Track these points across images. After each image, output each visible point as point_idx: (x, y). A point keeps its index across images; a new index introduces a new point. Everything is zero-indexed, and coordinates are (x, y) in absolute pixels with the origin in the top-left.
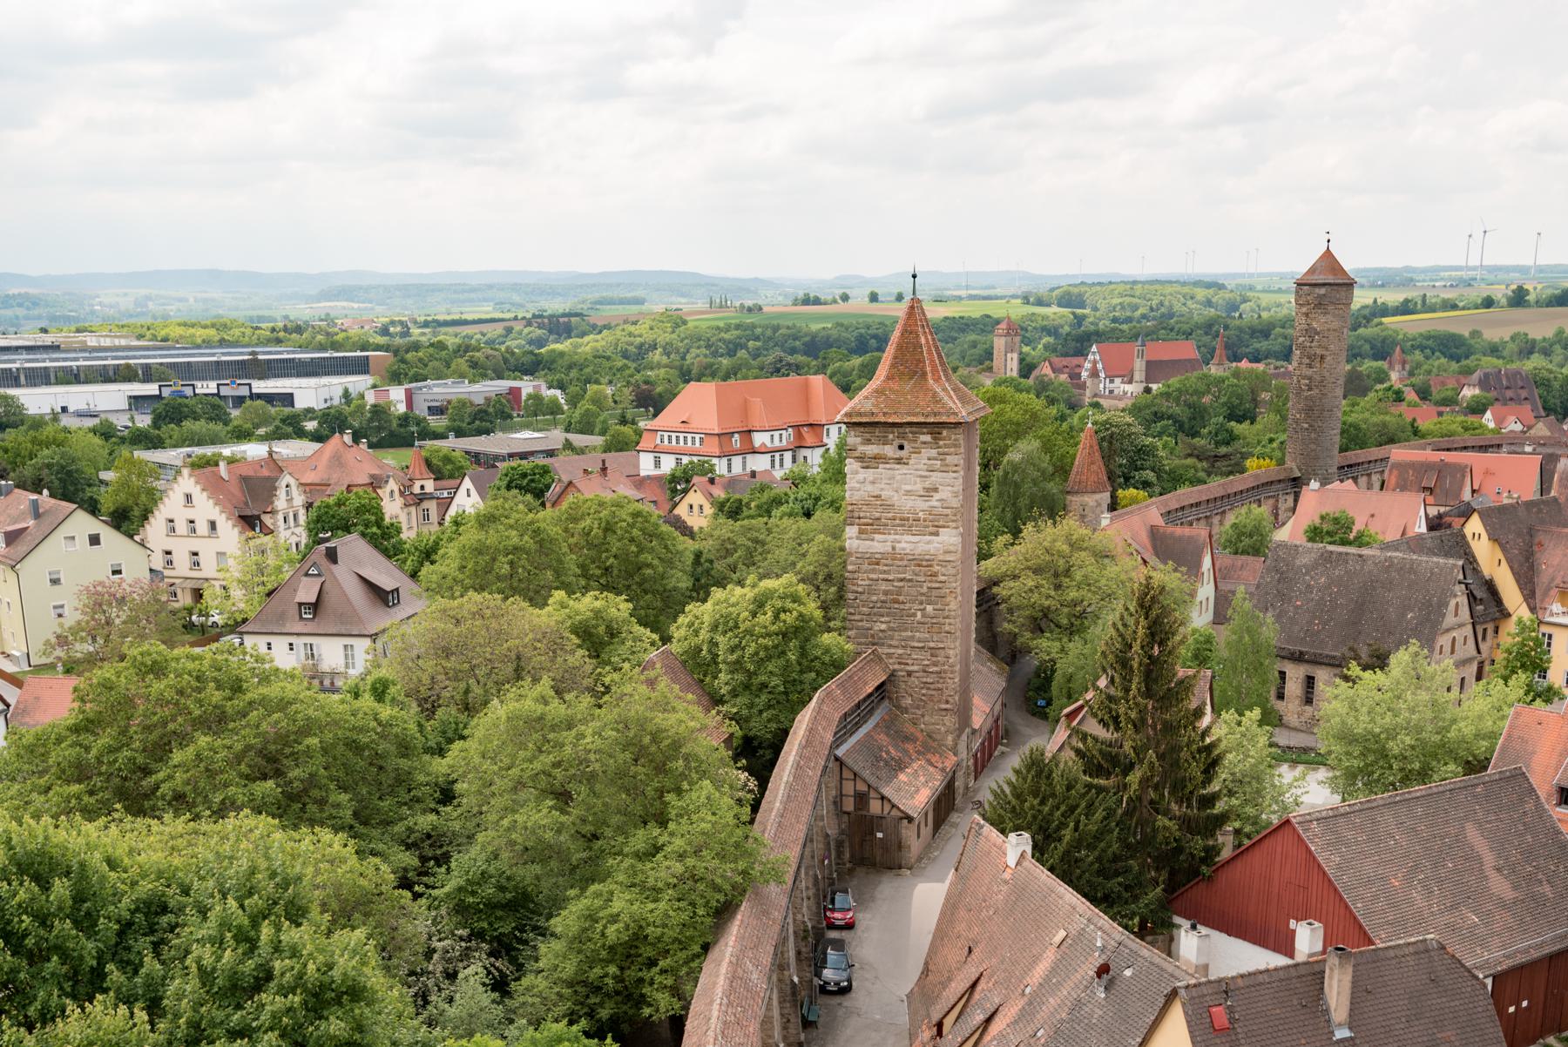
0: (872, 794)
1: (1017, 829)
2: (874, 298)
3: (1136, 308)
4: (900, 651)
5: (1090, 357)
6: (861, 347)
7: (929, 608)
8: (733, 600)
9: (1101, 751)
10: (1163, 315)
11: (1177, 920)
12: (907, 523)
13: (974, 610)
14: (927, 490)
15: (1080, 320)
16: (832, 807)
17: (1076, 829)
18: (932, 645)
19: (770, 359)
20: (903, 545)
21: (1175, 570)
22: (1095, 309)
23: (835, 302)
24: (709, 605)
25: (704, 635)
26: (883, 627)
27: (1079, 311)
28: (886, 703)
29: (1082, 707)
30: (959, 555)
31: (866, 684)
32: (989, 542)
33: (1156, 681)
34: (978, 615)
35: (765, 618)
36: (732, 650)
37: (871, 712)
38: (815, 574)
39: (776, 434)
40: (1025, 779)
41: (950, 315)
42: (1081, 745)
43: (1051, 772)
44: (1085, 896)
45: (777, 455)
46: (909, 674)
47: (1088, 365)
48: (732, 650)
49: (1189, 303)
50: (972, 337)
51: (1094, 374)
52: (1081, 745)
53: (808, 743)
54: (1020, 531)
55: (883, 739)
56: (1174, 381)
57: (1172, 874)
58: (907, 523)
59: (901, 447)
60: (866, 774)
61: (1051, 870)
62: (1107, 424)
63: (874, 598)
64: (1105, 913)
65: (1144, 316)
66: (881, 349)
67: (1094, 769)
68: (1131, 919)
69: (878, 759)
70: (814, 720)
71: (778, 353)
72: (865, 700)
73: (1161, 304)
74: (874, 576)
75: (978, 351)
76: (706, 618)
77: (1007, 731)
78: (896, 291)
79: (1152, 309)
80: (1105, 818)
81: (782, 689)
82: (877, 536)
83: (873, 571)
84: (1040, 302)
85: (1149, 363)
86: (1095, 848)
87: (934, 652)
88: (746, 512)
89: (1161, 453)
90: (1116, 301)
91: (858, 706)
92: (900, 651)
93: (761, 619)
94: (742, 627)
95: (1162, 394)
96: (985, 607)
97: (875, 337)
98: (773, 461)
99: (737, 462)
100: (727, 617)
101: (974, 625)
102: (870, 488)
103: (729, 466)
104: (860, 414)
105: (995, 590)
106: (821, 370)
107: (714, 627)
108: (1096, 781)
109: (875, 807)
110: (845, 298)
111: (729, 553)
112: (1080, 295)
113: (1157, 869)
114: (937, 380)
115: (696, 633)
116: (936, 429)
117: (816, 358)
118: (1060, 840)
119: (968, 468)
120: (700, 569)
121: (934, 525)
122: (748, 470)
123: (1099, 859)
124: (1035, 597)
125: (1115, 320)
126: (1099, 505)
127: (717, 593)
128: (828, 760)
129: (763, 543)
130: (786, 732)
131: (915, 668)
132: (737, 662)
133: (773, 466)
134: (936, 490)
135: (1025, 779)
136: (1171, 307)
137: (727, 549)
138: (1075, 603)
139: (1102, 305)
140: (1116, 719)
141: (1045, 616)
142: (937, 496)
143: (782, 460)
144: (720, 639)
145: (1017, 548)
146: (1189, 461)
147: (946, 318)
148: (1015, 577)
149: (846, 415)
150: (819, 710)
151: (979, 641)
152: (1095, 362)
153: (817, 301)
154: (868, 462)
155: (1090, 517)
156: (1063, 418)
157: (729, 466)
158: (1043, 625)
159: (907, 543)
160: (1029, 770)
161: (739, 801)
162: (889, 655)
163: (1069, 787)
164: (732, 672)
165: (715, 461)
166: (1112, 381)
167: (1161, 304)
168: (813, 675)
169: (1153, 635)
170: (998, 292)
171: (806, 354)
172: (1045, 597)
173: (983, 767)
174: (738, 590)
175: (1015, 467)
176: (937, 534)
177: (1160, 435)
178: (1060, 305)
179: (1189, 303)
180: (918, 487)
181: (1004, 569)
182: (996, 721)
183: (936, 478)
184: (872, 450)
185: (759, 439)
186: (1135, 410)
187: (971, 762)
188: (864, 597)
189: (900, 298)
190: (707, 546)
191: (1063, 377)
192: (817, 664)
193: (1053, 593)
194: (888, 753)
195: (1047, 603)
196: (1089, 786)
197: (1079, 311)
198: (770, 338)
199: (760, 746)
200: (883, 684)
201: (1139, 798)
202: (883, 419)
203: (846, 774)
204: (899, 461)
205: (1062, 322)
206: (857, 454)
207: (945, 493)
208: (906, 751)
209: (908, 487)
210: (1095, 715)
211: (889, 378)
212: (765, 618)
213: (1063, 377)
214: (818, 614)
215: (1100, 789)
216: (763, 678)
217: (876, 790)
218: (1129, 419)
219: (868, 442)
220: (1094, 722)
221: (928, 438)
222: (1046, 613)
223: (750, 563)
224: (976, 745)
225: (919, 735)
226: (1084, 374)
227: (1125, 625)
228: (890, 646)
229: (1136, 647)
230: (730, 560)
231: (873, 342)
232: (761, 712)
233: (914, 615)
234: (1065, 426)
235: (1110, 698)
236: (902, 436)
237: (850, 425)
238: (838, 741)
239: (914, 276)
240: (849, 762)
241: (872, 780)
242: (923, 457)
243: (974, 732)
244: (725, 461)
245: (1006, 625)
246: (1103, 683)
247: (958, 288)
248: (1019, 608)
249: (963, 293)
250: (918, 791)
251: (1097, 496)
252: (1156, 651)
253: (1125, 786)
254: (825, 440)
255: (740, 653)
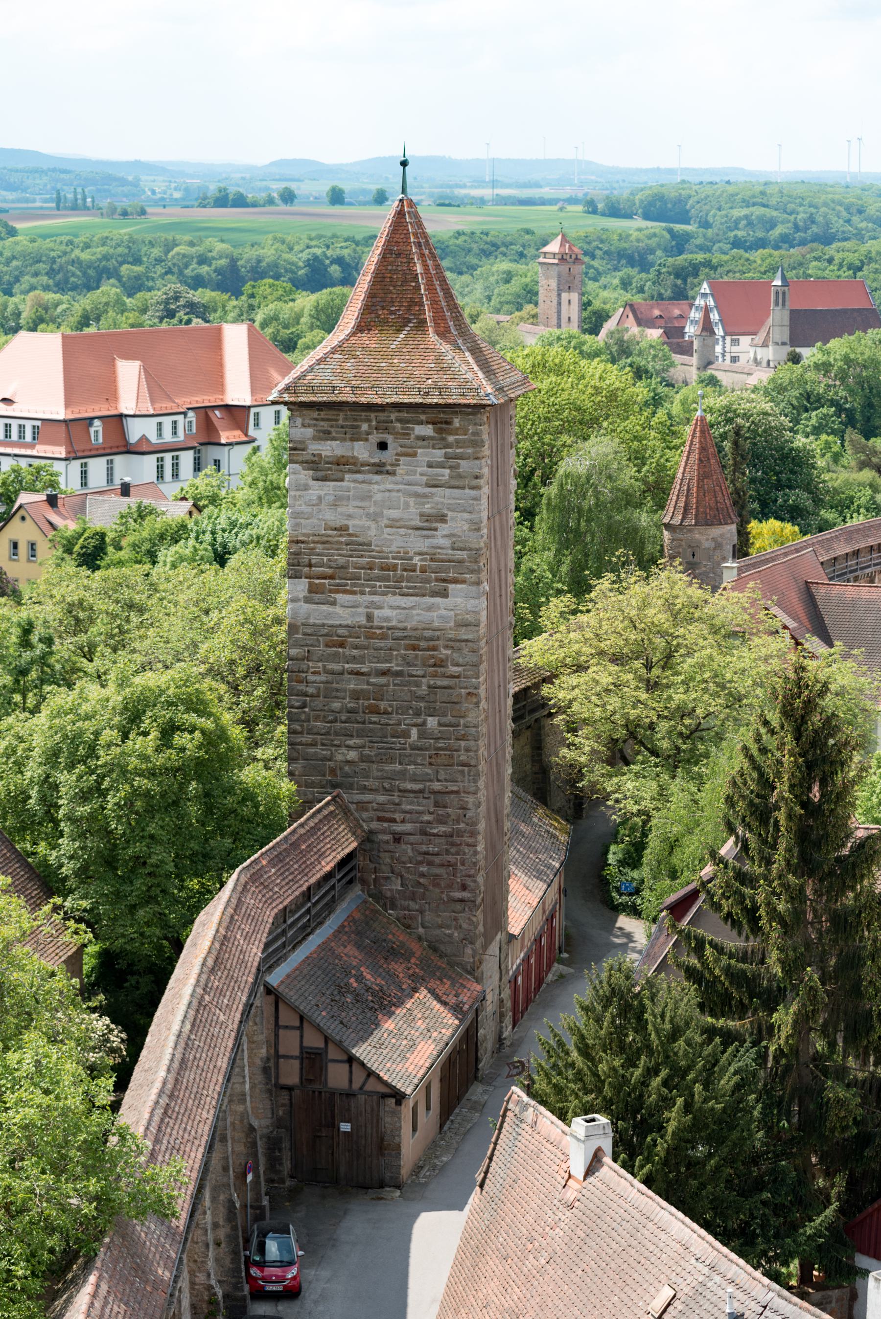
0: (333, 1053)
1: (587, 1110)
2: (337, 197)
3: (772, 224)
4: (381, 798)
5: (699, 302)
6: (315, 277)
7: (432, 722)
8: (86, 708)
9: (727, 970)
10: (816, 239)
11: (862, 1261)
12: (394, 575)
13: (510, 725)
14: (426, 517)
15: (679, 244)
16: (260, 1078)
17: (688, 1107)
18: (437, 786)
19: (158, 295)
20: (386, 612)
21: (846, 656)
22: (706, 225)
23: (270, 201)
24: (42, 719)
25: (33, 770)
26: (352, 755)
27: (679, 227)
28: (357, 891)
29: (693, 896)
30: (482, 630)
31: (322, 855)
32: (535, 608)
33: (817, 845)
34: (516, 734)
35: (144, 744)
36: (84, 797)
37: (330, 908)
38: (232, 662)
39: (167, 421)
40: (599, 1020)
41: (467, 229)
42: (694, 961)
43: (643, 1009)
44: (707, 1226)
45: (168, 457)
46: (398, 838)
47: (695, 315)
48: (84, 797)
49: (856, 219)
50: (505, 265)
51: (707, 327)
52: (694, 961)
53: (217, 963)
54: (589, 589)
55: (350, 953)
56: (838, 346)
57: (852, 1184)
58: (394, 575)
59: (383, 446)
60: (321, 1017)
61: (648, 1182)
62: (728, 414)
63: (336, 705)
64: (741, 1254)
65: (786, 240)
66: (348, 281)
67: (715, 1000)
68: (786, 1264)
69: (343, 989)
70: (230, 923)
71: (174, 285)
72: (319, 884)
73: (812, 220)
74: (331, 666)
75: (515, 286)
76: (38, 740)
77: (568, 937)
78: (374, 187)
79: (797, 228)
80: (738, 1087)
81: (171, 867)
82: (339, 596)
83: (335, 657)
84: (615, 211)
85: (792, 312)
86: (721, 1141)
87: (439, 799)
88: (111, 553)
89: (821, 463)
90: (738, 213)
91: (307, 895)
92: (381, 798)
93: (137, 743)
94: (104, 757)
95: (817, 366)
96: (529, 719)
97: (339, 261)
98: (160, 469)
99: (97, 467)
100: (75, 739)
101: (509, 752)
102: (331, 517)
103: (84, 474)
104: (312, 390)
105: (546, 690)
106: (246, 315)
107: (52, 757)
108: (721, 1022)
109: (337, 1076)
110: (288, 197)
111: (79, 626)
112: (680, 201)
113: (829, 1174)
114: (443, 334)
115: (20, 767)
116: (443, 416)
117: (237, 294)
118: (661, 1128)
119: (498, 481)
120: (27, 655)
121: (437, 576)
122: (117, 482)
123: (729, 1161)
124: (614, 702)
125: (737, 244)
126: (718, 546)
127: (60, 698)
128: (252, 993)
129: (141, 611)
130: (178, 946)
131: (408, 827)
132: (91, 817)
133: (160, 475)
134: (442, 518)
135: (599, 1020)
136: (828, 224)
137: (77, 617)
138: (683, 712)
139: (717, 218)
140: (752, 914)
141: (632, 735)
142: (444, 529)
143: (176, 466)
144: (66, 779)
145: (583, 618)
146: (868, 475)
147: (459, 233)
148: (580, 668)
149: (287, 389)
150: (237, 904)
151: (519, 780)
152: (707, 311)
153: (240, 202)
154: (324, 470)
155: (705, 565)
156: (656, 401)
157: (84, 474)
158: (628, 752)
159: (392, 609)
160: (607, 1002)
161: (93, 1071)
162: (362, 806)
163: (675, 1034)
164: (82, 836)
165: (59, 467)
166: (735, 342)
167: (812, 220)
168: (228, 841)
169: (810, 766)
170: (546, 192)
171: (220, 287)
172: (631, 701)
173: (528, 1001)
174: (94, 691)
175: (582, 485)
176: (444, 594)
177: (817, 431)
178: (647, 217)
179: (856, 219)
180: (412, 513)
181: (561, 654)
182: (550, 919)
183: (443, 497)
184: (330, 449)
185: (136, 430)
186: (777, 389)
187: (507, 993)
188: (319, 703)
189: (381, 198)
190: (47, 613)
191: (655, 334)
192: (231, 820)
193: (644, 696)
194: (360, 978)
195: (633, 713)
196: (710, 1032)
197: (679, 227)
198: (159, 261)
199: (131, 970)
200: (350, 856)
201: (795, 1051)
202: (351, 399)
203: (287, 1018)
204: (379, 469)
205: (653, 242)
206: (306, 456)
207: (458, 524)
208: (391, 976)
209: (394, 514)
210: (717, 907)
211: (361, 327)
212: (144, 744)
213: (655, 334)
214: (237, 733)
215: (729, 1037)
216: (138, 848)
217: (339, 1045)
218: (768, 407)
219: (325, 435)
220: (715, 918)
221: (427, 430)
222: (633, 729)
223: (118, 642)
224: (515, 961)
225: (414, 946)
226: (690, 330)
227: (763, 750)
228: (364, 789)
229: (782, 788)
230: (82, 638)
231: (335, 270)
232: (133, 908)
233: (406, 734)
234: (661, 415)
235: (742, 877)
236: (384, 427)
237: (296, 407)
238: (272, 958)
239: (404, 164)
240: (291, 995)
241: (333, 1029)
242: (420, 464)
243: (511, 937)
244: (76, 465)
245: (564, 751)
246: (728, 848)
247: (479, 183)
248: (585, 722)
249: (486, 193)
250: (413, 1046)
251: (716, 531)
252: (816, 793)
253: (771, 1027)
254: (252, 432)
255: (95, 804)
